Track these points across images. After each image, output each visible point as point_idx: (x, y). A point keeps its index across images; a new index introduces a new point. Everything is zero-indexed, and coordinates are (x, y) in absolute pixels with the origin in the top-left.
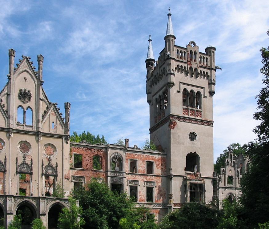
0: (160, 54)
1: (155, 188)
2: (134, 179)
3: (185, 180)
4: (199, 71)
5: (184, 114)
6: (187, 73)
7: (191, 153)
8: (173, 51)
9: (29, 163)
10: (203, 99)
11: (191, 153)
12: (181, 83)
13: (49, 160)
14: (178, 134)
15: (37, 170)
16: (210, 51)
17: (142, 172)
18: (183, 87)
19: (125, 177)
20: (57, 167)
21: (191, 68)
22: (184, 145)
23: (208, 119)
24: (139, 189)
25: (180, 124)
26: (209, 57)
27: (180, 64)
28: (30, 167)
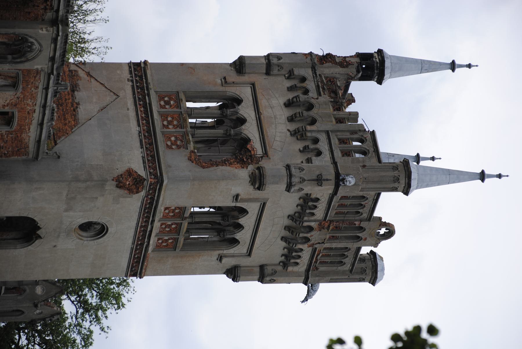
0: (373, 133)
7: (39, 228)
10: (217, 253)
11: (39, 228)
12: (264, 204)
22: (66, 210)
23: (150, 264)
26: (347, 267)
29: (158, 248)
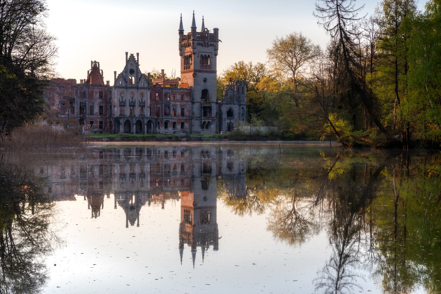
1: (185, 109)
3: (201, 104)
4: (209, 44)
9: (134, 101)
13: (142, 99)
15: (137, 104)
16: (216, 30)
18: (200, 54)
20: (145, 102)
24: (177, 109)
28: (135, 103)
29: (210, 69)
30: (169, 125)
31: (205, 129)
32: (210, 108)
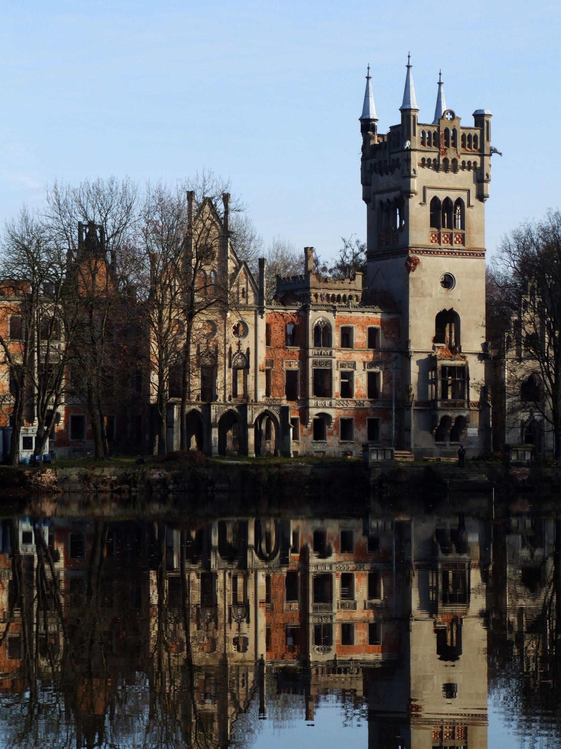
2: (347, 358)
4: (460, 163)
5: (432, 242)
6: (437, 168)
8: (415, 135)
14: (423, 279)
17: (361, 346)
18: (431, 194)
19: (335, 358)
21: (446, 160)
25: (425, 260)
27: (427, 155)
30: (328, 429)
31: (448, 443)
32: (463, 371)
